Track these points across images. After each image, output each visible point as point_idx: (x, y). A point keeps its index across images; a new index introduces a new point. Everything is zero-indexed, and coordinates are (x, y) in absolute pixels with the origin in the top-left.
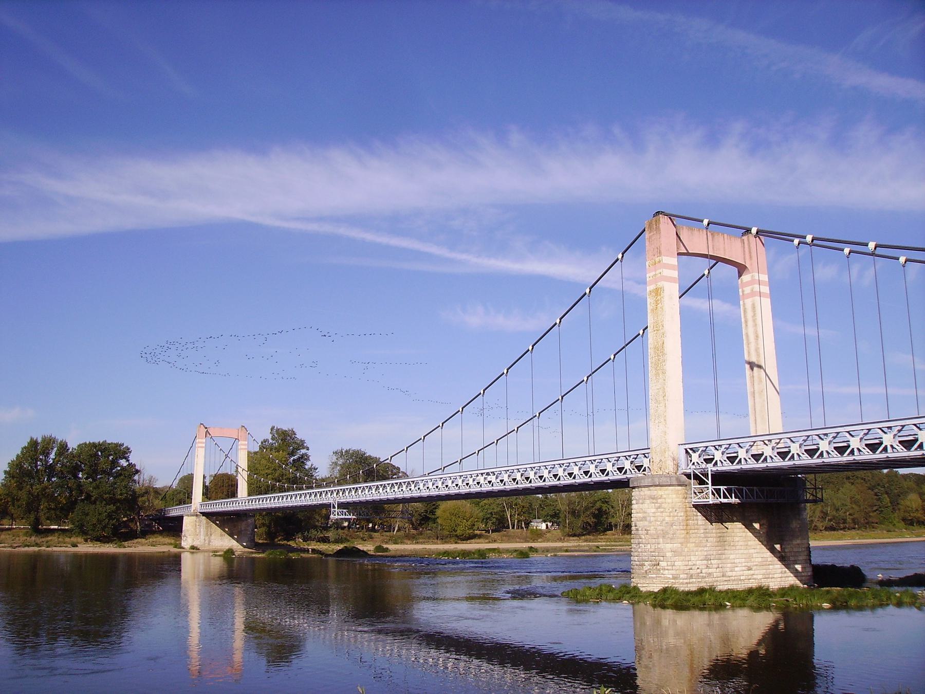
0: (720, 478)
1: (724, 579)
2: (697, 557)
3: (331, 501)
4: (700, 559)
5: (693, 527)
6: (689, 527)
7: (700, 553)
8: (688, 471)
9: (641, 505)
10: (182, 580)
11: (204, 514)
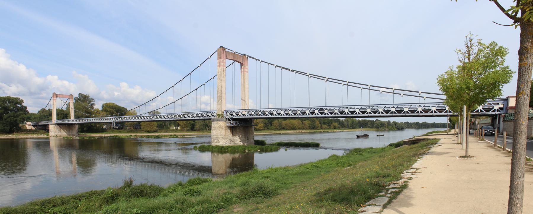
0: (234, 119)
3: (112, 121)
8: (227, 117)
9: (214, 126)
10: (51, 147)
11: (58, 124)
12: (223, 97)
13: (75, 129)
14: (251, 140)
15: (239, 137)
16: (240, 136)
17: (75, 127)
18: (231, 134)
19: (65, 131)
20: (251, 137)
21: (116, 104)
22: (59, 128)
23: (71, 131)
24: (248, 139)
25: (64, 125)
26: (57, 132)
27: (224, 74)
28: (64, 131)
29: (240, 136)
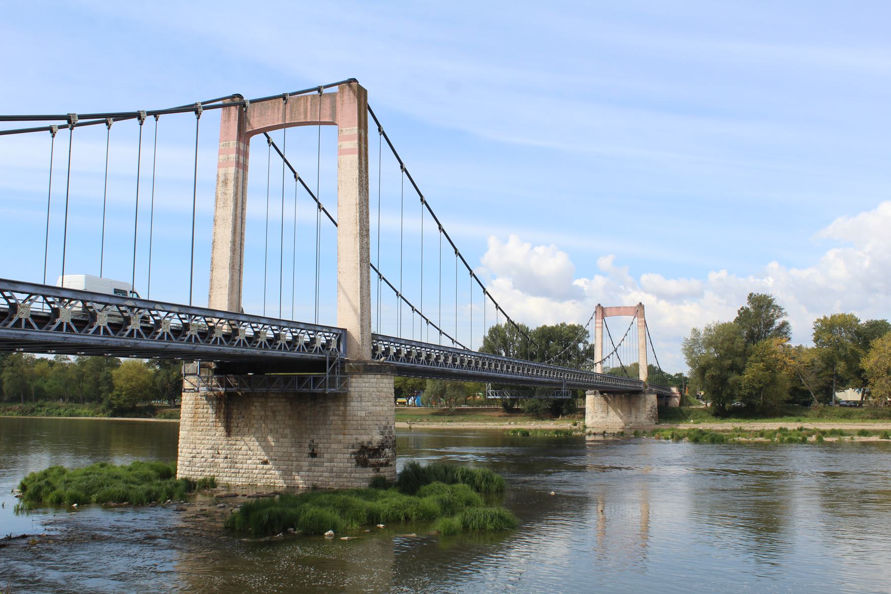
1: (233, 470)
2: (203, 446)
4: (206, 448)
5: (201, 416)
7: (206, 442)
12: (215, 282)
14: (331, 461)
15: (262, 441)
16: (270, 438)
17: (645, 401)
18: (222, 428)
19: (620, 411)
20: (334, 446)
21: (568, 324)
22: (604, 402)
23: (633, 412)
24: (313, 455)
25: (618, 396)
26: (600, 415)
27: (225, 194)
28: (616, 411)
29: (270, 438)
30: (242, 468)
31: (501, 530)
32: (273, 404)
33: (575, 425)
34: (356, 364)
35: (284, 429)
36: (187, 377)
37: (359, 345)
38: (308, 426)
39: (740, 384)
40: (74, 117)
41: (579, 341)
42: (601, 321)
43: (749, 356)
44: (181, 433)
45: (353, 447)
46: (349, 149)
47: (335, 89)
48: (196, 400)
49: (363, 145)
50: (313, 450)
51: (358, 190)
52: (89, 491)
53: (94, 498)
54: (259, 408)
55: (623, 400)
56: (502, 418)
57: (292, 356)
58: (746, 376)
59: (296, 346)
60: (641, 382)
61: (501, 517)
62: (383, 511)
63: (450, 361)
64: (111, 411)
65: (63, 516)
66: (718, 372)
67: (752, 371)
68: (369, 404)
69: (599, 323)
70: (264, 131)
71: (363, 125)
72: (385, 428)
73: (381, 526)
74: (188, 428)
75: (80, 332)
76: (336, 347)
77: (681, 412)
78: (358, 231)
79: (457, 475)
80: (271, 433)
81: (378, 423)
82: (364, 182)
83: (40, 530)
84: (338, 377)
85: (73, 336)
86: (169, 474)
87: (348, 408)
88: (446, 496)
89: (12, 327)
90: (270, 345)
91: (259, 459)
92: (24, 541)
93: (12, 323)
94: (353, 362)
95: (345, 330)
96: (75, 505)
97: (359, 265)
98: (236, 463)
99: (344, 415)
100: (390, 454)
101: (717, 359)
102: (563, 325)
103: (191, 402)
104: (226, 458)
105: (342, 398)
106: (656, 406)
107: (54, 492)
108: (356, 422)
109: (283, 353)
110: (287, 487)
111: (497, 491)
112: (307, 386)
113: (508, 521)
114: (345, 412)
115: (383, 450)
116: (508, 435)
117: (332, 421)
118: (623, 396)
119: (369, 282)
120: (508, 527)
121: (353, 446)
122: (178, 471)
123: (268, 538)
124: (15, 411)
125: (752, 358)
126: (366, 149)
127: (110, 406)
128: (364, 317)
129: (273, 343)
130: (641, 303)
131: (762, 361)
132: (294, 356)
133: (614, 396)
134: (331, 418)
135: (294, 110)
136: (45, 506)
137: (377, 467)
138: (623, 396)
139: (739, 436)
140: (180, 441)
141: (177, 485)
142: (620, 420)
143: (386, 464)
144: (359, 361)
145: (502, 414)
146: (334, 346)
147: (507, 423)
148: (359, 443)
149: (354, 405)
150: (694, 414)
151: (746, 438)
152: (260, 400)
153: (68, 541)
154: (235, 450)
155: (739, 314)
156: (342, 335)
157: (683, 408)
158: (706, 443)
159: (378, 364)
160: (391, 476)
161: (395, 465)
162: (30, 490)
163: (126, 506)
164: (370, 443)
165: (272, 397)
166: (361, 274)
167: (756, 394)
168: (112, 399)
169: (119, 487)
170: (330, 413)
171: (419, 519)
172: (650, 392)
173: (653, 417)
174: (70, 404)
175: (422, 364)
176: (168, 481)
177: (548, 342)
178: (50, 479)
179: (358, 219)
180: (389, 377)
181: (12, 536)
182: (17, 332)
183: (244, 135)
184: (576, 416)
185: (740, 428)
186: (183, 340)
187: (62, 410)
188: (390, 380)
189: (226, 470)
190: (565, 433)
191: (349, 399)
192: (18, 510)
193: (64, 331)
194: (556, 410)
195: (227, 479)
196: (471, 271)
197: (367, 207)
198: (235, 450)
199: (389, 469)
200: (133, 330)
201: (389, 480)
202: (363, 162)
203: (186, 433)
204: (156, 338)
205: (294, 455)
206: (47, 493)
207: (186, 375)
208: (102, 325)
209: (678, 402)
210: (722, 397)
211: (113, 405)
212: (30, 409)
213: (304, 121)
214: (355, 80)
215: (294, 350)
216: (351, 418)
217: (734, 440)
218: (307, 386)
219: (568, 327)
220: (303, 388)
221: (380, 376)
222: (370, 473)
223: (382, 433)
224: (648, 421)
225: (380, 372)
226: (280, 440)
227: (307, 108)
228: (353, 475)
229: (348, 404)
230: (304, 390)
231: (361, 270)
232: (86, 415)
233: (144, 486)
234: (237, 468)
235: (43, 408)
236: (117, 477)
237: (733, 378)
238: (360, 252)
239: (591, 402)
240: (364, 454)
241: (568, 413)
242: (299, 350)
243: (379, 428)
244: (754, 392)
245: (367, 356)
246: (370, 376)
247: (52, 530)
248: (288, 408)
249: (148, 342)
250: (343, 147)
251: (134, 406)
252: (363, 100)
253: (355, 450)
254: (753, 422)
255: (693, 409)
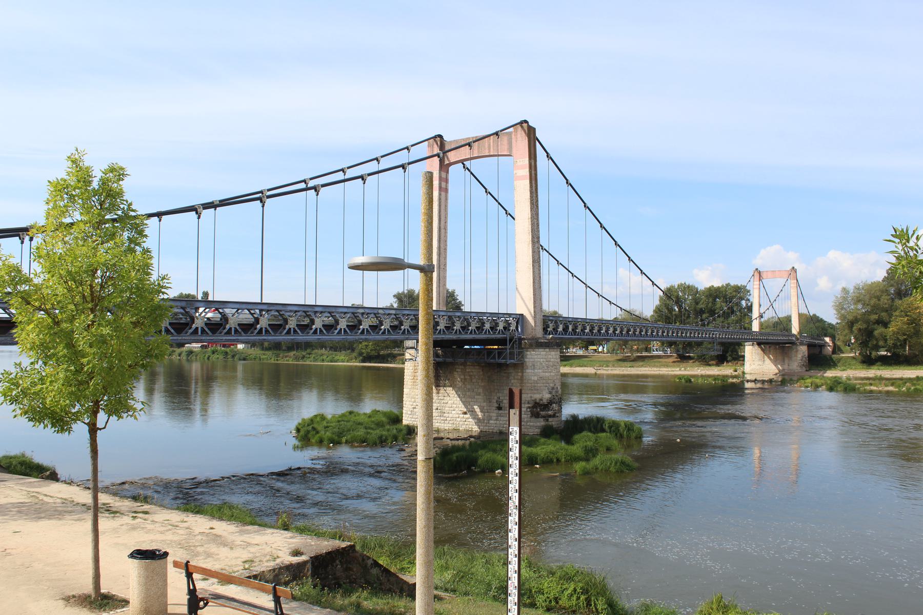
1: (442, 418)
6: (416, 378)
13: (797, 356)
17: (797, 351)
23: (786, 361)
26: (757, 363)
30: (448, 417)
31: (622, 472)
32: (470, 370)
33: (736, 371)
34: (530, 341)
35: (478, 388)
36: (408, 351)
37: (532, 326)
38: (496, 387)
39: (885, 336)
40: (319, 187)
41: (742, 299)
42: (758, 283)
43: (895, 311)
44: (405, 390)
45: (528, 403)
46: (523, 176)
47: (511, 129)
48: (415, 366)
49: (533, 172)
50: (499, 405)
51: (529, 208)
52: (340, 434)
53: (344, 440)
54: (460, 373)
55: (778, 351)
56: (675, 364)
57: (480, 338)
58: (891, 329)
59: (483, 330)
60: (794, 335)
61: (623, 463)
62: (540, 455)
63: (611, 331)
64: (361, 358)
65: (323, 452)
66: (864, 326)
67: (897, 324)
68: (540, 371)
69: (756, 285)
70: (462, 161)
71: (532, 156)
72: (553, 388)
73: (538, 466)
74: (410, 387)
75: (328, 333)
76: (515, 328)
77: (831, 359)
78: (531, 239)
79: (605, 425)
80: (469, 391)
81: (547, 385)
82: (535, 201)
83: (309, 464)
84: (516, 351)
85: (324, 337)
86: (397, 420)
87: (525, 374)
88: (590, 444)
89: (285, 334)
90: (463, 330)
91: (461, 411)
92: (299, 472)
93: (285, 331)
94: (528, 339)
95: (522, 315)
96: (331, 445)
97: (532, 265)
98: (444, 413)
99: (522, 379)
100: (557, 408)
101: (864, 314)
102: (728, 285)
103: (411, 368)
104: (437, 409)
105: (520, 366)
106: (807, 355)
107: (318, 435)
108: (530, 385)
109: (473, 336)
110: (481, 431)
111: (636, 438)
112: (494, 358)
113: (628, 465)
114: (522, 376)
115: (551, 405)
116: (675, 381)
117: (513, 384)
118: (777, 347)
119: (540, 277)
120: (627, 469)
121: (528, 402)
122: (403, 418)
123: (456, 474)
124: (290, 357)
125: (897, 313)
126: (536, 175)
127: (361, 354)
128: (536, 305)
129: (466, 329)
130: (793, 268)
131: (907, 316)
132: (482, 338)
133: (770, 347)
134: (512, 381)
135: (480, 146)
136: (312, 445)
137: (546, 418)
138: (777, 347)
139: (871, 384)
140: (404, 396)
141: (401, 430)
142: (774, 367)
143: (554, 416)
144: (533, 339)
145: (676, 360)
146: (513, 327)
147: (678, 369)
148: (533, 400)
149: (529, 371)
150: (844, 361)
151: (877, 387)
152: (460, 367)
153: (326, 472)
154: (443, 403)
155: (887, 273)
156: (520, 319)
157: (834, 356)
158: (840, 391)
159: (547, 341)
160: (558, 424)
161: (561, 416)
162: (302, 433)
163: (365, 447)
164: (541, 400)
165: (469, 365)
166: (533, 272)
167: (901, 345)
168: (362, 349)
169: (361, 432)
170: (511, 378)
171: (567, 461)
172: (802, 344)
173: (803, 365)
174: (331, 352)
175: (587, 335)
176: (395, 427)
177: (714, 300)
178: (315, 426)
179: (530, 229)
180: (555, 350)
181: (292, 468)
182: (289, 338)
183: (444, 167)
184: (739, 362)
185: (881, 376)
186: (399, 333)
187: (325, 357)
188: (556, 353)
189: (437, 418)
190: (722, 380)
191: (525, 368)
192: (295, 448)
193: (318, 334)
194: (721, 360)
195: (438, 424)
196: (629, 257)
197: (538, 220)
198: (443, 403)
199: (555, 419)
200: (364, 329)
201: (555, 428)
202: (534, 185)
203: (408, 390)
204: (380, 333)
205: (485, 408)
206: (314, 436)
207: (406, 349)
208: (343, 328)
209: (831, 350)
210: (869, 347)
211: (363, 353)
212: (301, 356)
213: (488, 154)
214: (526, 122)
215: (482, 333)
216: (527, 381)
217: (865, 390)
218: (494, 358)
219: (733, 287)
220: (491, 359)
221: (548, 350)
222: (541, 423)
223: (550, 393)
224: (799, 368)
225: (548, 347)
226: (476, 397)
227: (490, 144)
228: (528, 423)
229: (524, 371)
230: (492, 361)
231: (533, 269)
232: (345, 362)
233: (378, 431)
234: (445, 417)
235: (311, 355)
236: (360, 424)
237: (879, 331)
238: (533, 255)
239: (750, 351)
240: (537, 408)
241: (732, 360)
242: (486, 333)
243: (548, 388)
244: (899, 344)
245: (539, 333)
246: (540, 350)
247: (316, 464)
248: (481, 373)
249: (374, 337)
250: (517, 175)
251: (379, 354)
252: (532, 136)
253: (530, 405)
254: (896, 369)
255: (843, 357)
